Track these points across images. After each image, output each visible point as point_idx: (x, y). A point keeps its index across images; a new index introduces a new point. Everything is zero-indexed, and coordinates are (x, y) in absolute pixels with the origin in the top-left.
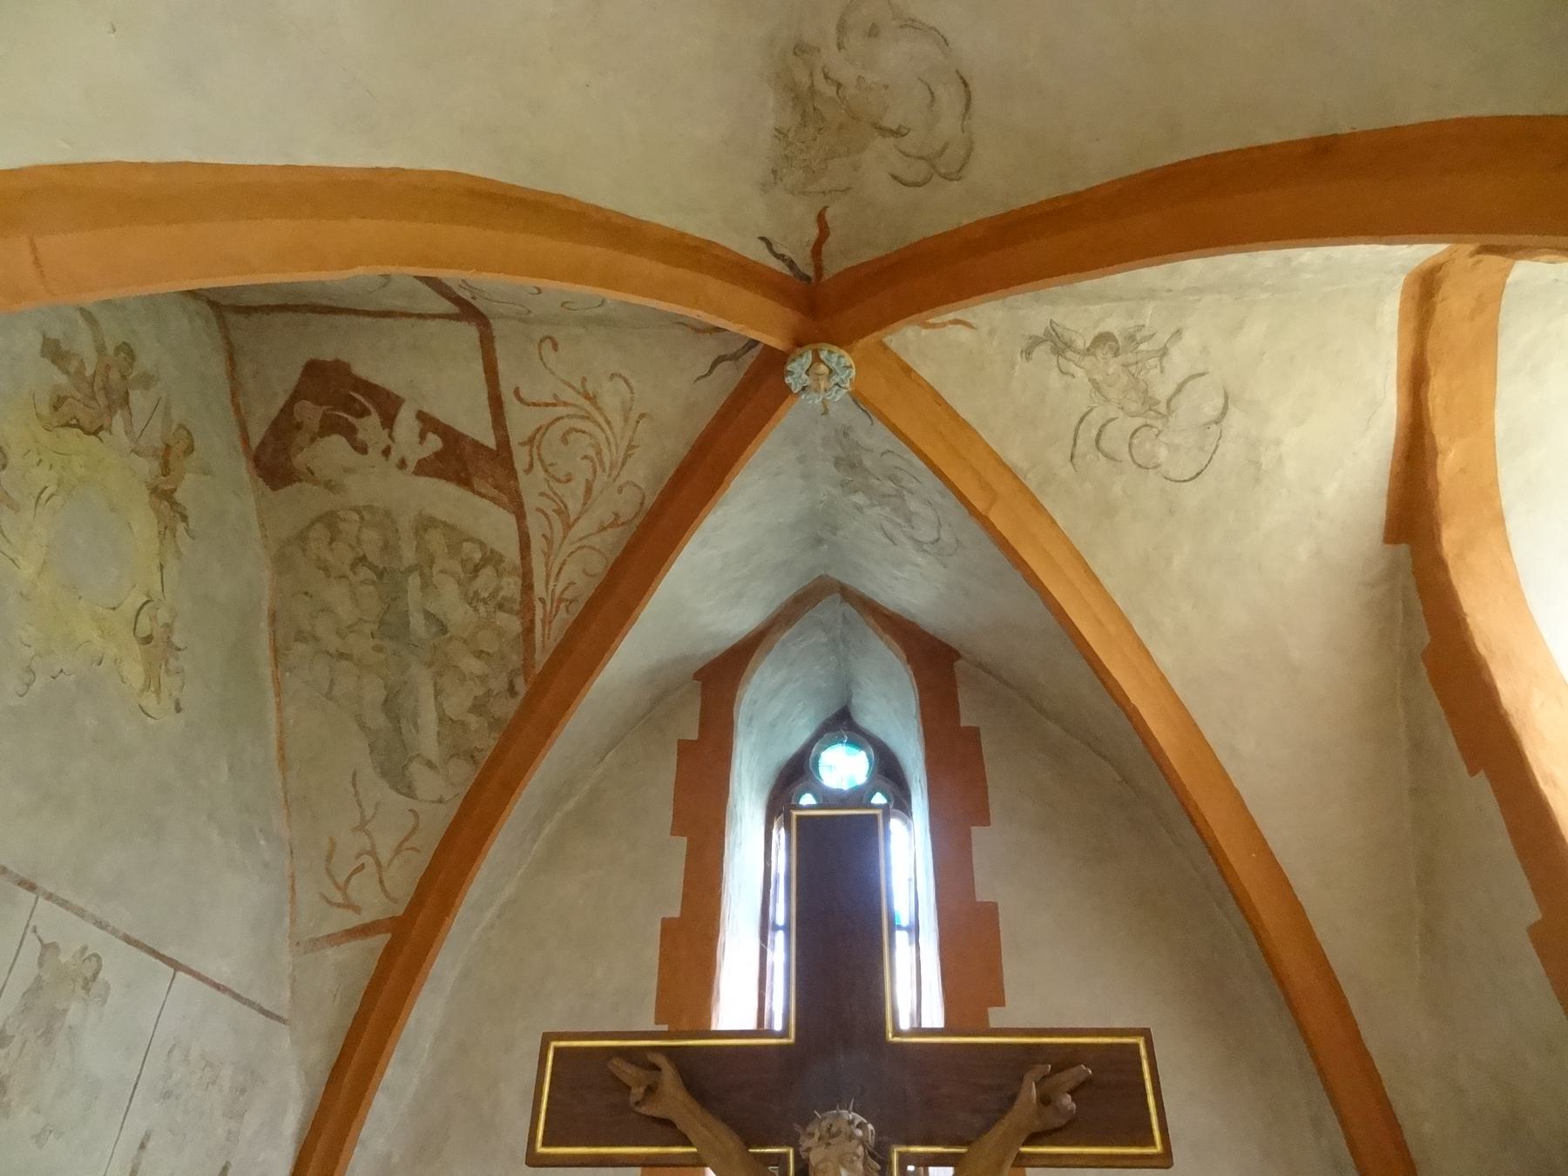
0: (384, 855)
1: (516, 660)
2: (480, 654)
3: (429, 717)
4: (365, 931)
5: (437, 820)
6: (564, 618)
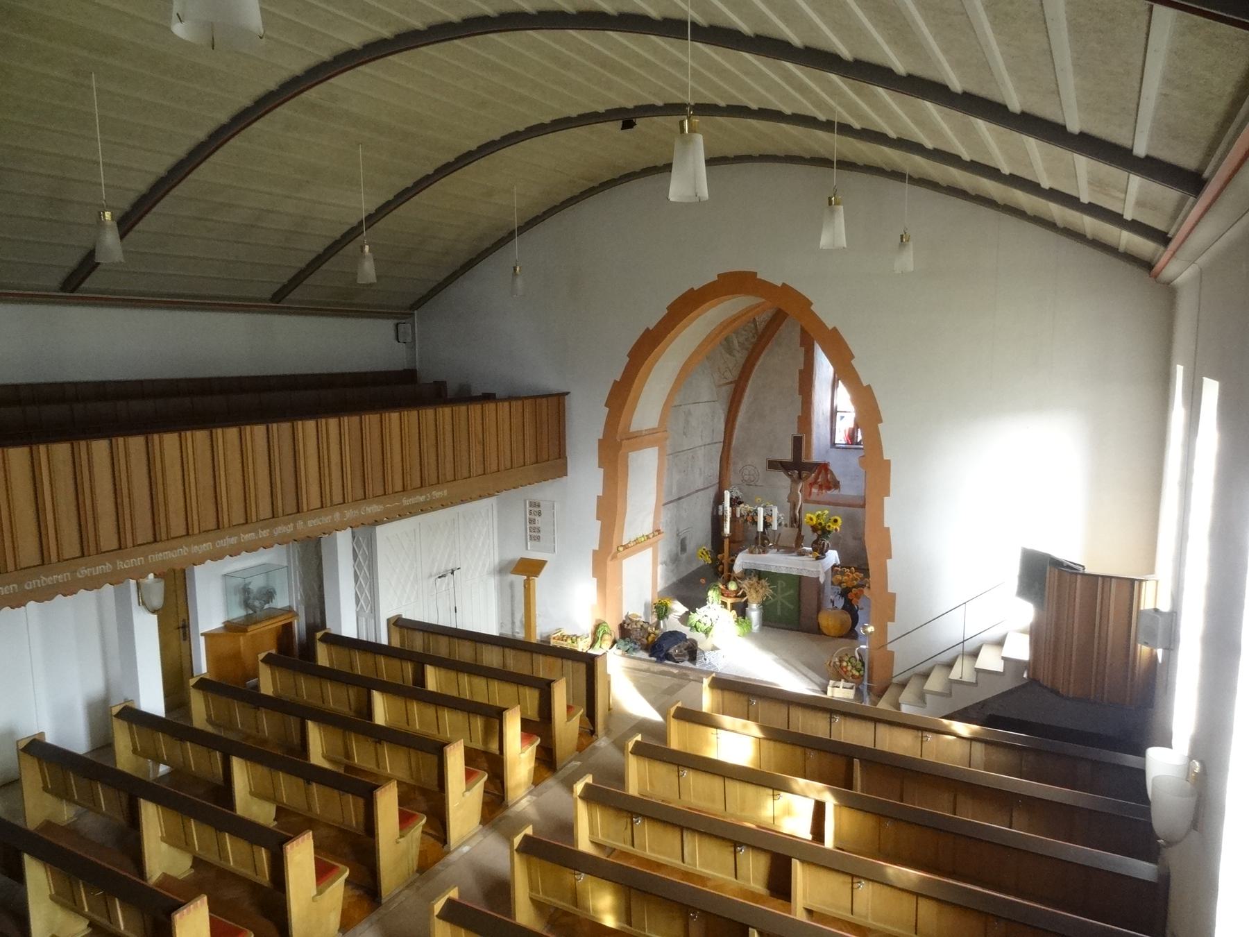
0: (731, 368)
1: (754, 331)
2: (746, 331)
3: (736, 342)
4: (731, 382)
5: (742, 361)
6: (763, 325)
